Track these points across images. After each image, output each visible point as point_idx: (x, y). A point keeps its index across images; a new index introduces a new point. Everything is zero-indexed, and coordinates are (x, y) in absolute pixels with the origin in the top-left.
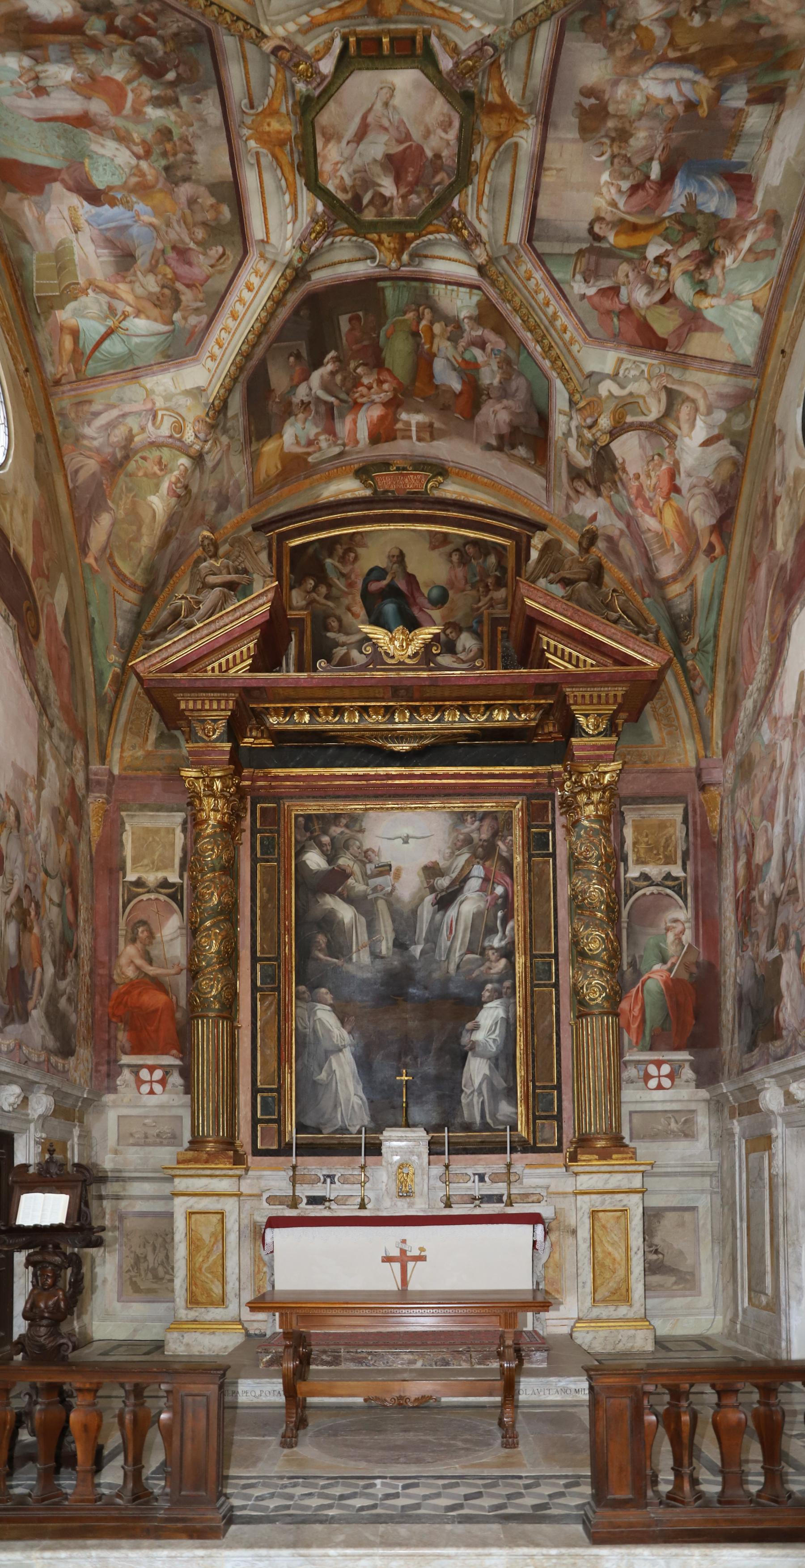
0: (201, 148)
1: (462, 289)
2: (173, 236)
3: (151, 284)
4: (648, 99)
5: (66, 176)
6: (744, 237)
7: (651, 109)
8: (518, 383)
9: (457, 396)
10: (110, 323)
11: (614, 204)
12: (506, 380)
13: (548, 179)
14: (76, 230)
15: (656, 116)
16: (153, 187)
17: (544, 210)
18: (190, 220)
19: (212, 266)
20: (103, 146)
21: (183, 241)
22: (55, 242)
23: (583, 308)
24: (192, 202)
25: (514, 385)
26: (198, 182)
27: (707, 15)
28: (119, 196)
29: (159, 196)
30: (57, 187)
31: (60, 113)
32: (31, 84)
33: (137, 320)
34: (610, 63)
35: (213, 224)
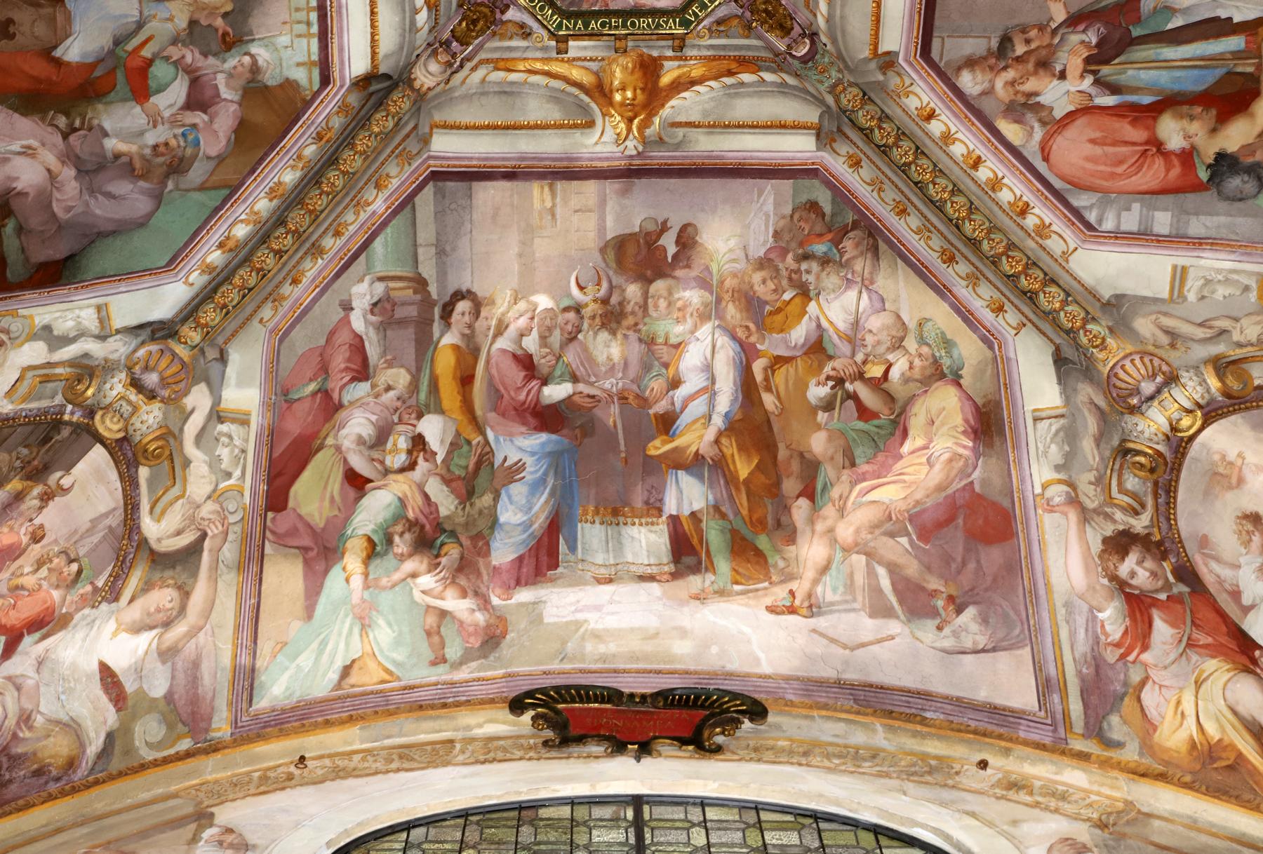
1: (315, 43)
4: (677, 346)
6: (464, 594)
7: (657, 355)
8: (131, 198)
9: (47, 53)
11: (500, 330)
12: (127, 167)
13: (538, 192)
15: (646, 367)
17: (488, 194)
23: (328, 312)
25: (122, 187)
34: (741, 266)
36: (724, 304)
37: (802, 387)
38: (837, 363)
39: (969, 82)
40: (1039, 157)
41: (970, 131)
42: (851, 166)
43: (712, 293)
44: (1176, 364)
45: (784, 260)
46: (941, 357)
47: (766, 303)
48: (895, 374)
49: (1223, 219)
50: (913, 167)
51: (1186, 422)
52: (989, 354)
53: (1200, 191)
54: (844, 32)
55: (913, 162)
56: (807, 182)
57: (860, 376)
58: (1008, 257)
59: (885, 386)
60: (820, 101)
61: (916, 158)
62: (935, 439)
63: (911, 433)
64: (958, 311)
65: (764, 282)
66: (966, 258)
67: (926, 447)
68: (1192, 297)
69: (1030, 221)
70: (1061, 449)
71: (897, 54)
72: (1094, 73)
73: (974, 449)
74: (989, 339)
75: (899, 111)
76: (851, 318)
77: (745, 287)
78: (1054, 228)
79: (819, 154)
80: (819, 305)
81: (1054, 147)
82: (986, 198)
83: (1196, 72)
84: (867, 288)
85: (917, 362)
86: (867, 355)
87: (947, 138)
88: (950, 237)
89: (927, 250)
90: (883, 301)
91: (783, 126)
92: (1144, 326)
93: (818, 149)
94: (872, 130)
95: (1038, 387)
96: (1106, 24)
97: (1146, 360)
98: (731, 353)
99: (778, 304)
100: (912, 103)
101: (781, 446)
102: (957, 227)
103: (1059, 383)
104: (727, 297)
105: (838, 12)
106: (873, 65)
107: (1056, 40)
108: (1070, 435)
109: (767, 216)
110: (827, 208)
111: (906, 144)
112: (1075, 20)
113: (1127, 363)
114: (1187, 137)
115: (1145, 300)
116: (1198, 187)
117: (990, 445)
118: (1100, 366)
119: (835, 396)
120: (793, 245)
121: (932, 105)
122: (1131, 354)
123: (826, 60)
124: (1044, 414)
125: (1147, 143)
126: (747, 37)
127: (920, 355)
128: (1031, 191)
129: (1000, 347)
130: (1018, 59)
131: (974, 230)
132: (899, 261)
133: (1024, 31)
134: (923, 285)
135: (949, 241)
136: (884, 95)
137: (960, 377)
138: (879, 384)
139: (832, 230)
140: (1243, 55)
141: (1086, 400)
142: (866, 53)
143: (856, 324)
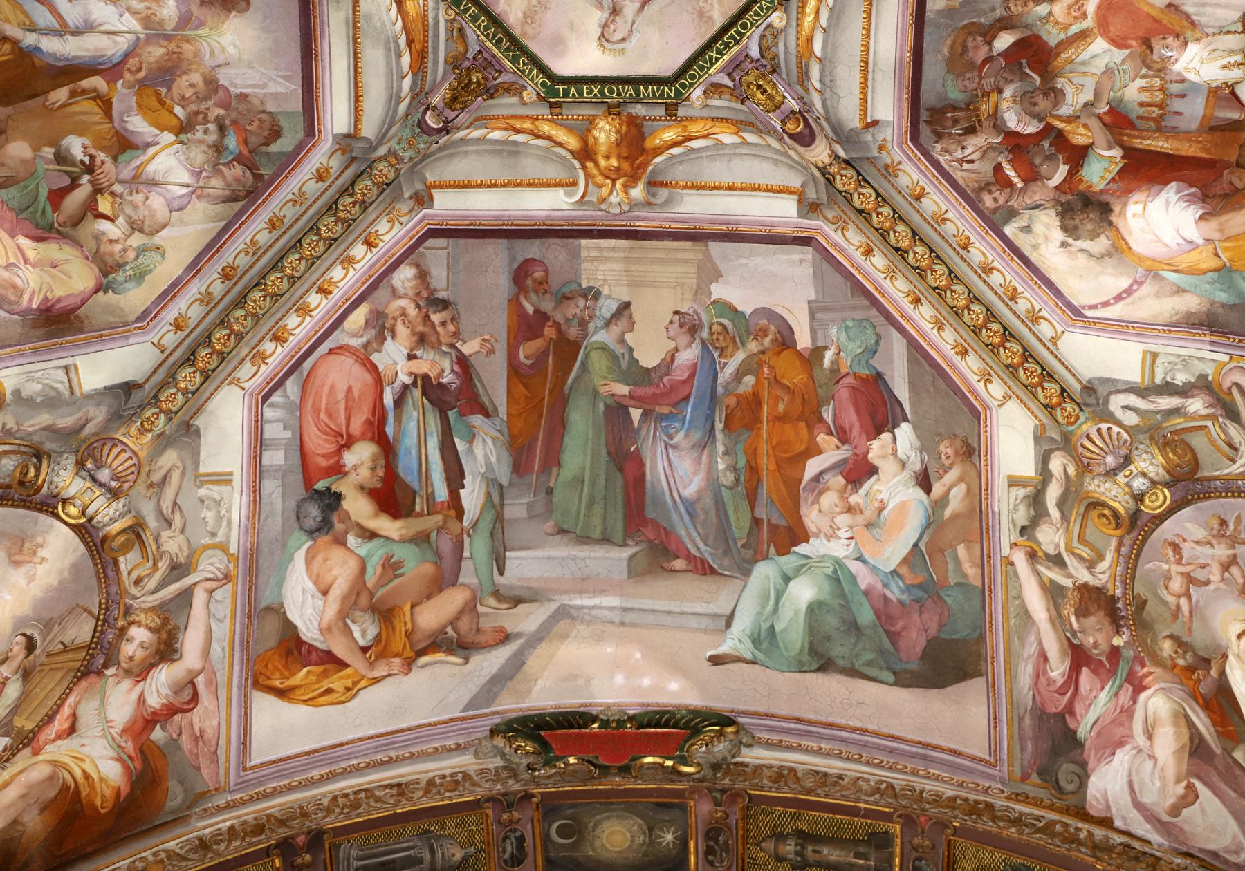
27: (62, 158)
36: (165, 43)
37: (80, 131)
38: (109, 165)
39: (405, 276)
40: (333, 345)
41: (357, 281)
42: (318, 170)
43: (174, 30)
44: (133, 493)
45: (216, 105)
46: (125, 271)
47: (169, 89)
48: (104, 225)
49: (279, 506)
50: (316, 238)
51: (73, 510)
52: (132, 318)
53: (305, 484)
54: (452, 155)
55: (321, 238)
56: (300, 126)
57: (98, 190)
58: (229, 335)
59: (89, 216)
60: (382, 138)
61: (325, 240)
62: (37, 270)
63: (40, 245)
64: (174, 285)
65: (192, 85)
66: (228, 292)
67: (26, 261)
68: (202, 492)
69: (268, 346)
70: (38, 394)
71: (431, 207)
72: (414, 384)
73: (29, 310)
74: (147, 317)
75: (373, 217)
76: (159, 178)
77: (185, 66)
78: (263, 367)
79: (330, 138)
80: (172, 144)
81: (343, 358)
82: (289, 305)
83: (416, 466)
84: (193, 192)
85: (118, 247)
86: (121, 196)
87: (348, 262)
88: (248, 276)
89: (234, 253)
90: (181, 209)
91: (357, 99)
92: (170, 458)
93: (335, 136)
94: (352, 195)
95: (100, 368)
96: (460, 389)
97: (133, 469)
98: (109, 53)
99: (168, 102)
100: (382, 226)
101: (9, 110)
102: (257, 284)
103: (105, 388)
104: (172, 46)
105: (471, 148)
106: (419, 186)
107: (444, 348)
108: (52, 401)
109: (263, 86)
110: (273, 148)
111: (339, 228)
112: (463, 363)
113: (128, 454)
114: (355, 467)
115: (197, 454)
116: (308, 482)
117: (35, 325)
118: (123, 430)
119: (74, 164)
120: (234, 115)
121: (381, 244)
122: (137, 456)
123: (422, 146)
124: (72, 375)
125: (349, 435)
126: (446, 61)
127: (125, 250)
128: (299, 343)
129: (139, 328)
130: (427, 317)
131: (255, 301)
132: (223, 223)
133: (453, 319)
134: (199, 248)
135: (244, 274)
136: (389, 200)
137: (106, 292)
138: (91, 209)
139: (252, 154)
140: (431, 502)
141: (90, 415)
142: (431, 178)
143: (153, 183)
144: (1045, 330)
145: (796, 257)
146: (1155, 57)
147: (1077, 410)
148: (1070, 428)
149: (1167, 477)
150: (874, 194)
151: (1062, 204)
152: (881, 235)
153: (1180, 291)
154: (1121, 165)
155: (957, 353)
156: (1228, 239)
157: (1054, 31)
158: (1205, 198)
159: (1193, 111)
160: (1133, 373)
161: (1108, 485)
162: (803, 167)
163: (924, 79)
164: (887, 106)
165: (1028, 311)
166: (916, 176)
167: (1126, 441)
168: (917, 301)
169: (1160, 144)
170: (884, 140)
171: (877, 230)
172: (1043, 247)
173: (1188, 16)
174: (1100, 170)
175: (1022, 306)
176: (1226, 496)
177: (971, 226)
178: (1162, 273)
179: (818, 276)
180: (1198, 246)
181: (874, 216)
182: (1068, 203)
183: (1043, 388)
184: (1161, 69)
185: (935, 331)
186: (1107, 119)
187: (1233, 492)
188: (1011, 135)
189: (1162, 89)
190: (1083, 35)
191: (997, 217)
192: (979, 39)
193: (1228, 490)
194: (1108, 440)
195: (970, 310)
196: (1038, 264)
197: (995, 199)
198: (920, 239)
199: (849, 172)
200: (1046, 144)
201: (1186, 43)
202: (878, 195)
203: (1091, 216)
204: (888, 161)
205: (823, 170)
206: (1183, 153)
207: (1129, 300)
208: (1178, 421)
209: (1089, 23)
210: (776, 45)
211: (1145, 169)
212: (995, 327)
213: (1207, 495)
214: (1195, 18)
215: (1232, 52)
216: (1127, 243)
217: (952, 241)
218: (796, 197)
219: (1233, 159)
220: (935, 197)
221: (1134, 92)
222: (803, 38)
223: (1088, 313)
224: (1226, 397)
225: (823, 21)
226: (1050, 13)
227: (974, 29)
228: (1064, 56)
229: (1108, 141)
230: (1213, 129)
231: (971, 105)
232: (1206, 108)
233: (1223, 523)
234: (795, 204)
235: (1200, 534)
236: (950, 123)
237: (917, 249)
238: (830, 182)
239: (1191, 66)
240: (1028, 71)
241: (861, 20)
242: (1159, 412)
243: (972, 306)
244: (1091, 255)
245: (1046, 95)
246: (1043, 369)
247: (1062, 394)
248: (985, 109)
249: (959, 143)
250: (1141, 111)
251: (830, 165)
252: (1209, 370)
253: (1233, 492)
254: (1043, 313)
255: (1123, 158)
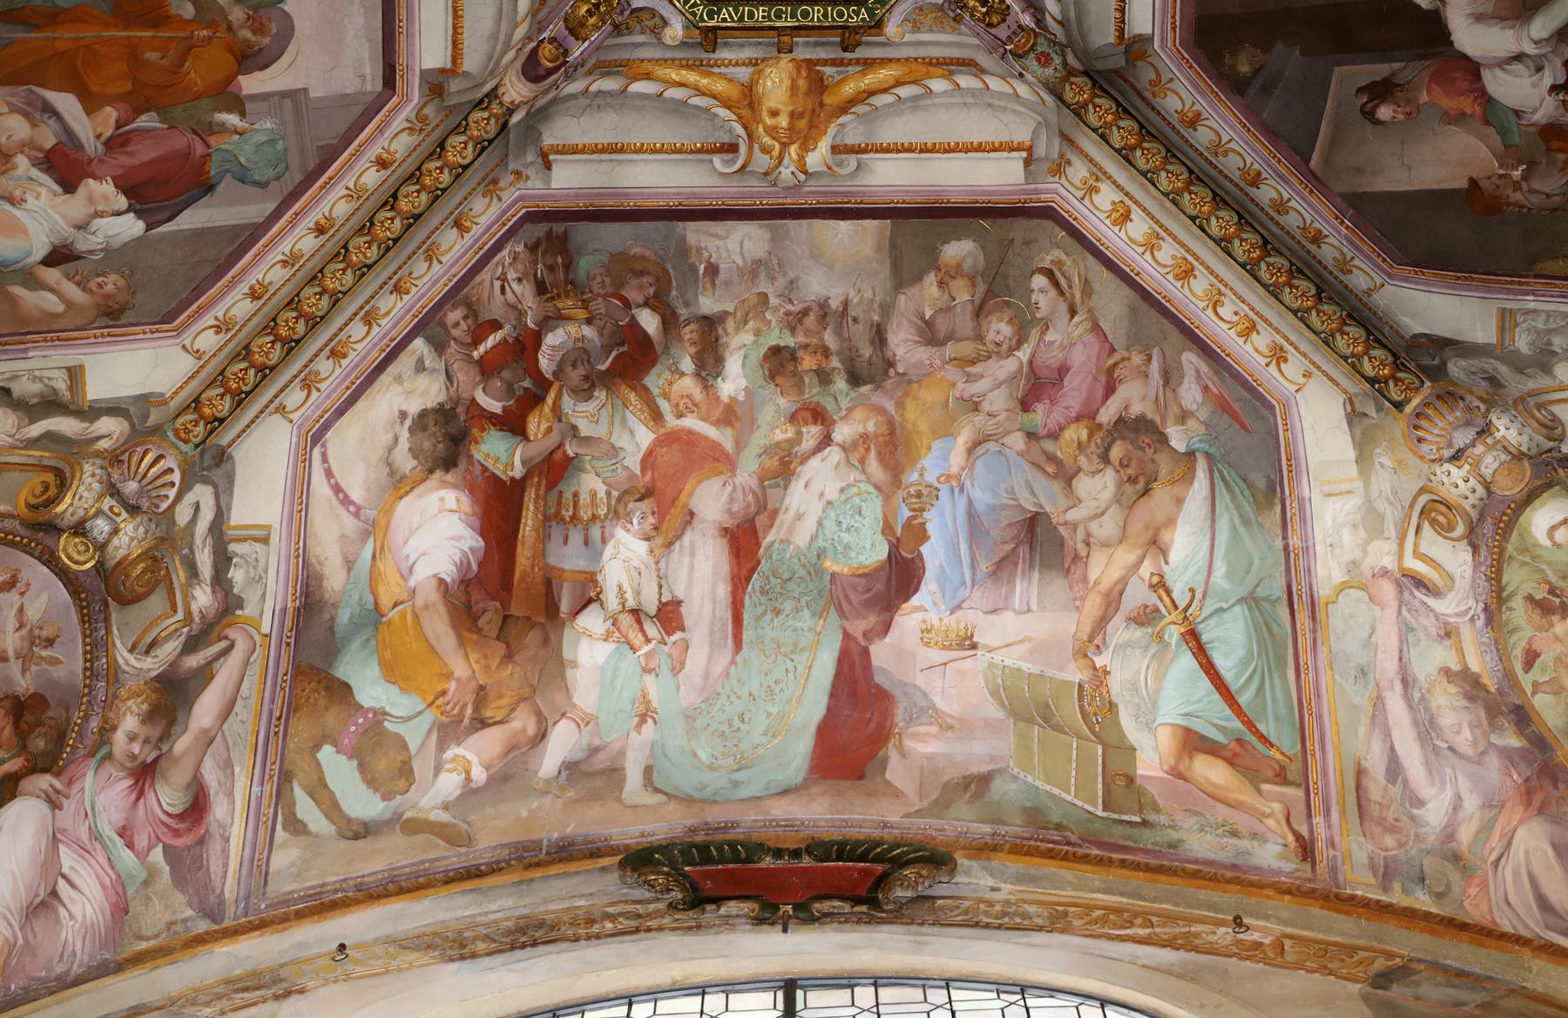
0: (816, 285)
2: (998, 401)
3: (1097, 487)
5: (858, 627)
10: (1174, 634)
14: (968, 644)
16: (891, 422)
18: (967, 348)
19: (1073, 312)
20: (799, 517)
21: (1014, 377)
22: (994, 711)
24: (930, 334)
26: (886, 309)
28: (906, 513)
29: (916, 416)
30: (880, 653)
31: (723, 590)
32: (652, 630)
33: (1173, 557)
35: (981, 288)
144: (294, 397)
145: (367, 70)
146: (631, 505)
147: (197, 440)
148: (170, 434)
149: (113, 562)
150: (466, 162)
151: (453, 409)
152: (413, 175)
153: (349, 564)
154: (503, 477)
155: (252, 288)
156: (416, 616)
157: (661, 381)
158: (465, 582)
159: (568, 557)
160: (242, 514)
161: (96, 486)
162: (493, 66)
163: (603, 225)
164: (570, 179)
165: (317, 373)
166: (483, 221)
167: (157, 507)
168: (320, 230)
169: (530, 523)
170: (528, 178)
171: (419, 168)
172: (397, 389)
173: (679, 537)
174: (498, 453)
175: (324, 366)
176: (85, 644)
177: (423, 296)
178: (371, 540)
179: (342, 101)
180: (406, 580)
181: (438, 164)
182: (456, 416)
183: (222, 395)
184: (617, 513)
185: (280, 257)
186: (558, 456)
187: (91, 652)
188: (537, 338)
189: (594, 517)
190: (657, 416)
191: (434, 329)
192: (651, 291)
193: (94, 645)
194: (158, 482)
195: (321, 294)
196: (377, 385)
197: (457, 324)
198: (410, 225)
199: (493, 128)
200: (527, 383)
201: (648, 539)
202: (465, 167)
203: (440, 446)
204: (502, 184)
205: (493, 94)
206: (519, 550)
207: (336, 503)
208: (182, 575)
209: (671, 422)
210: (643, 33)
211: (499, 508)
212: (301, 327)
213: (86, 619)
214: (677, 545)
215: (638, 593)
216: (407, 493)
217: (403, 272)
218: (449, 66)
219: (513, 611)
220: (459, 247)
221: (591, 484)
222: (650, 67)
223: (317, 452)
224: (215, 634)
225: (672, 93)
226: (682, 374)
227: (663, 281)
228: (632, 396)
229: (532, 459)
230: (548, 583)
231: (572, 286)
232: (574, 572)
233: (50, 642)
234: (439, 65)
235: (34, 613)
236: (550, 261)
237: (398, 222)
238: (478, 104)
239: (622, 549)
240: (614, 354)
241: (672, 141)
242: (192, 551)
243: (326, 298)
244: (390, 450)
245: (586, 378)
246: (248, 393)
247: (216, 419)
248: (566, 305)
249: (525, 274)
250: (568, 496)
251: (501, 104)
252: (249, 610)
253: (91, 652)
254: (315, 394)
255: (513, 479)
